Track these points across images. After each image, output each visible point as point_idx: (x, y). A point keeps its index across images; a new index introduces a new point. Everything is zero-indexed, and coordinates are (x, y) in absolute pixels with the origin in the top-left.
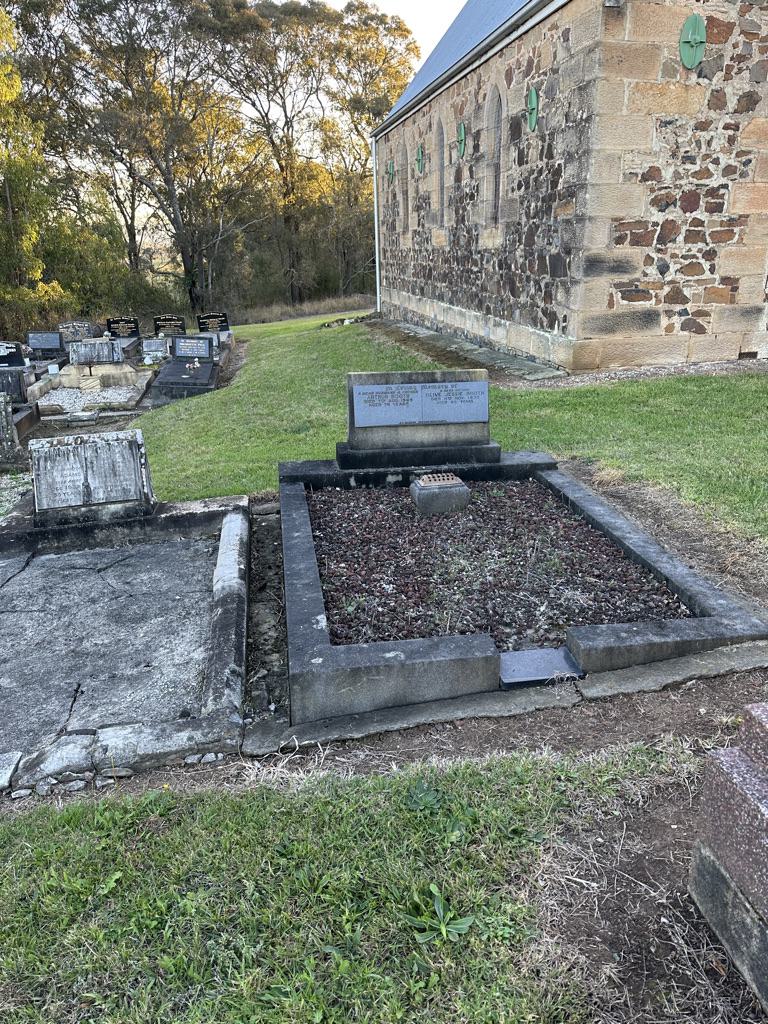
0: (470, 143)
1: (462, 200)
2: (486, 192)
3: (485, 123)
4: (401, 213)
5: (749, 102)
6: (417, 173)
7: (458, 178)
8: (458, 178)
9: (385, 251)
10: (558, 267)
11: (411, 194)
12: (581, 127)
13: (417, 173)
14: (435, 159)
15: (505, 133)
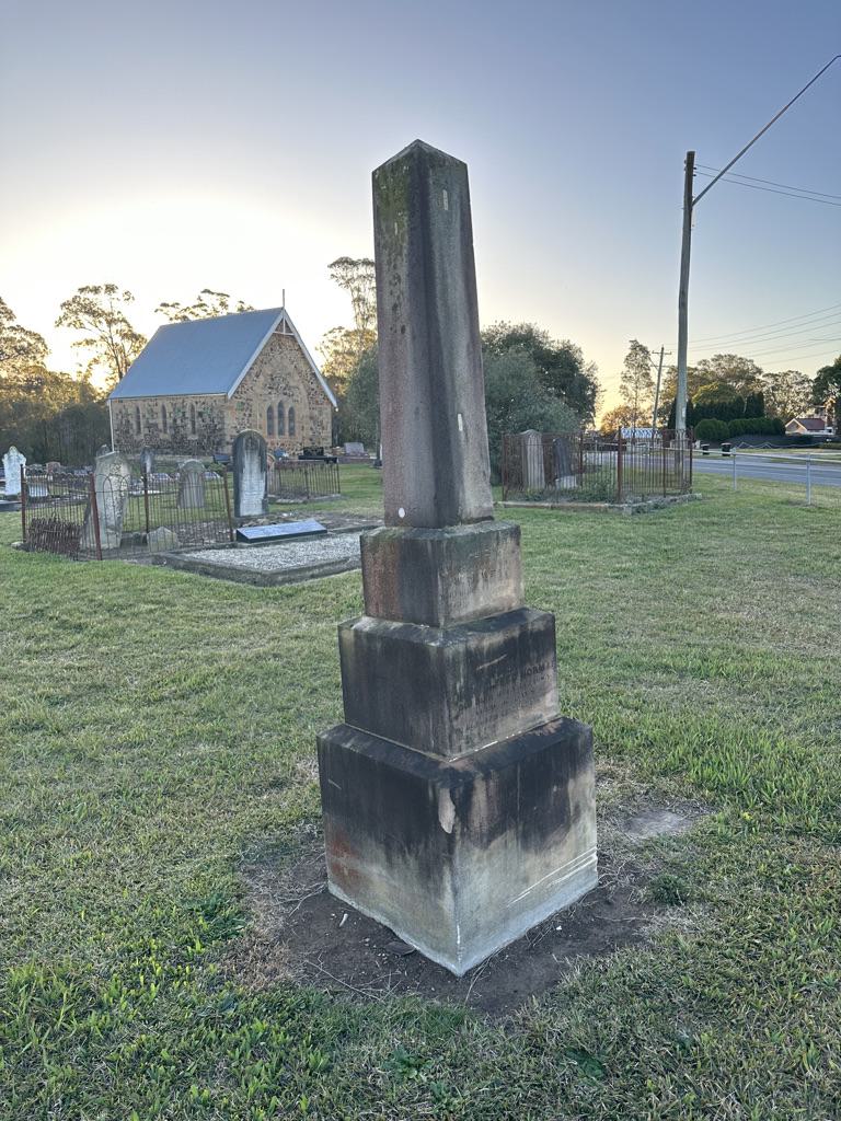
0: (181, 415)
1: (175, 427)
2: (189, 426)
3: (188, 409)
4: (135, 427)
5: (250, 415)
6: (147, 416)
7: (175, 421)
8: (175, 421)
9: (118, 441)
10: (219, 443)
11: (142, 421)
12: (222, 418)
13: (147, 416)
14: (160, 415)
15: (196, 414)
